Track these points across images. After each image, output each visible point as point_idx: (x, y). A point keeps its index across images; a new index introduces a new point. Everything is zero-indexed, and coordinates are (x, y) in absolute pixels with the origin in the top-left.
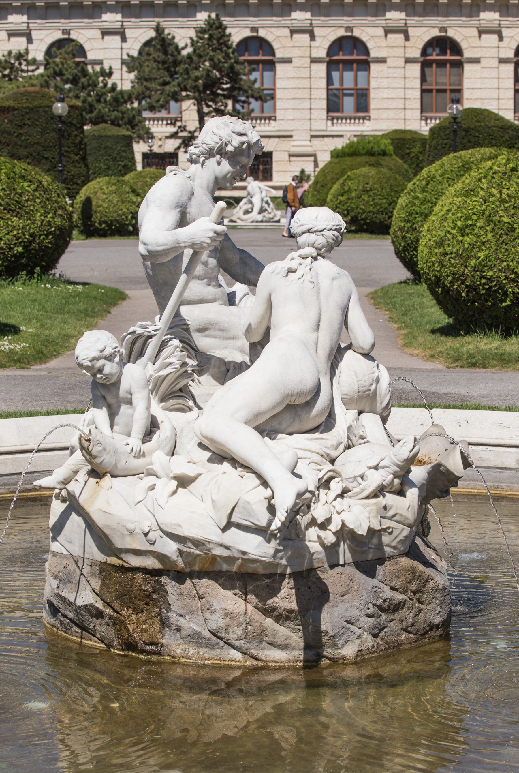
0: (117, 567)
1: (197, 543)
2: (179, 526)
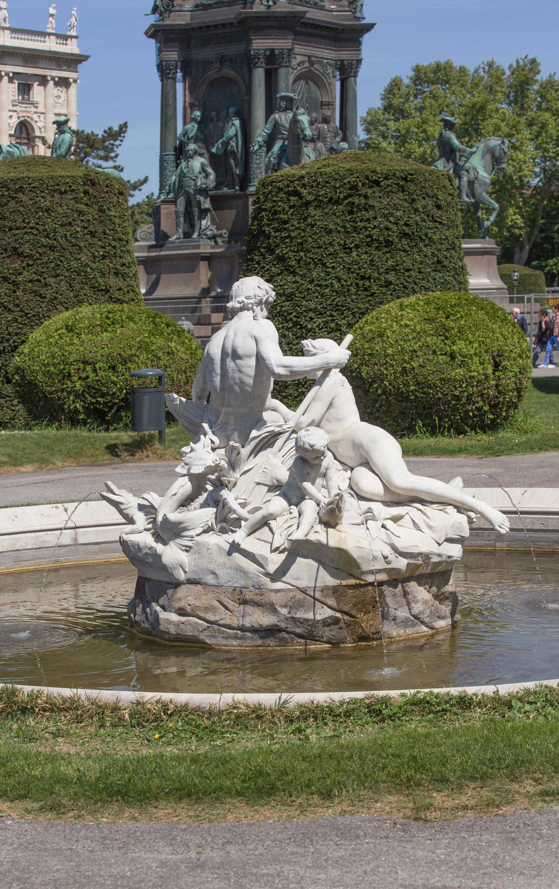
0: (353, 586)
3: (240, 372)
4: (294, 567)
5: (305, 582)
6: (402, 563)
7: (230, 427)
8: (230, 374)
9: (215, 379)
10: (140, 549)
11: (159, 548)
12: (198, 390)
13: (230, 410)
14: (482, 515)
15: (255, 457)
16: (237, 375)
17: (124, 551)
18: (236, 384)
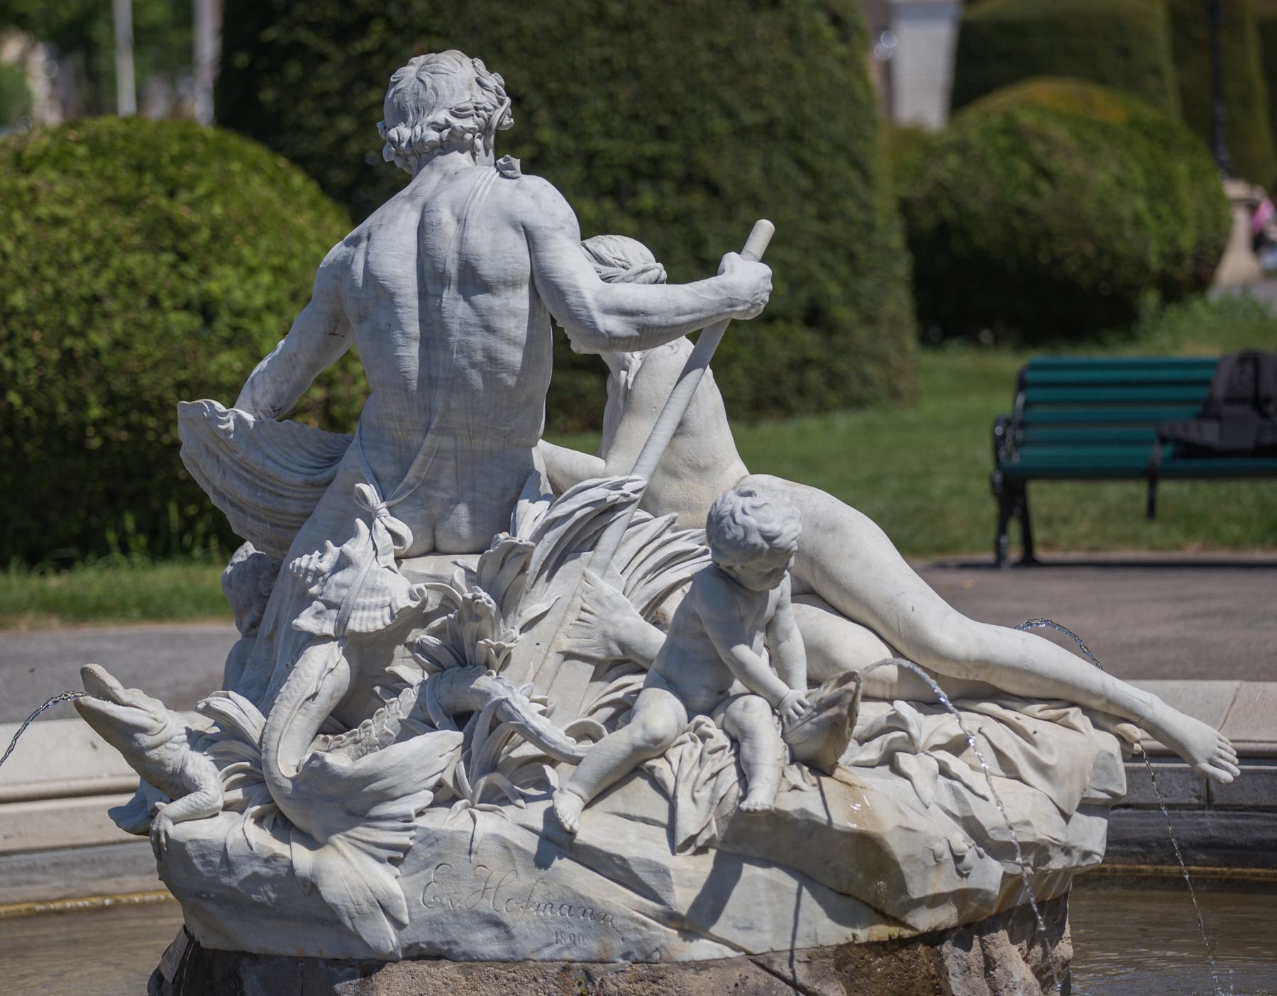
1: (1040, 850)
2: (1027, 823)
3: (489, 329)
4: (738, 892)
5: (764, 940)
6: (990, 875)
7: (441, 495)
8: (456, 337)
9: (402, 352)
10: (228, 863)
11: (302, 857)
12: (285, 387)
13: (446, 442)
14: (1154, 729)
15: (549, 579)
16: (478, 339)
17: (165, 874)
18: (473, 365)
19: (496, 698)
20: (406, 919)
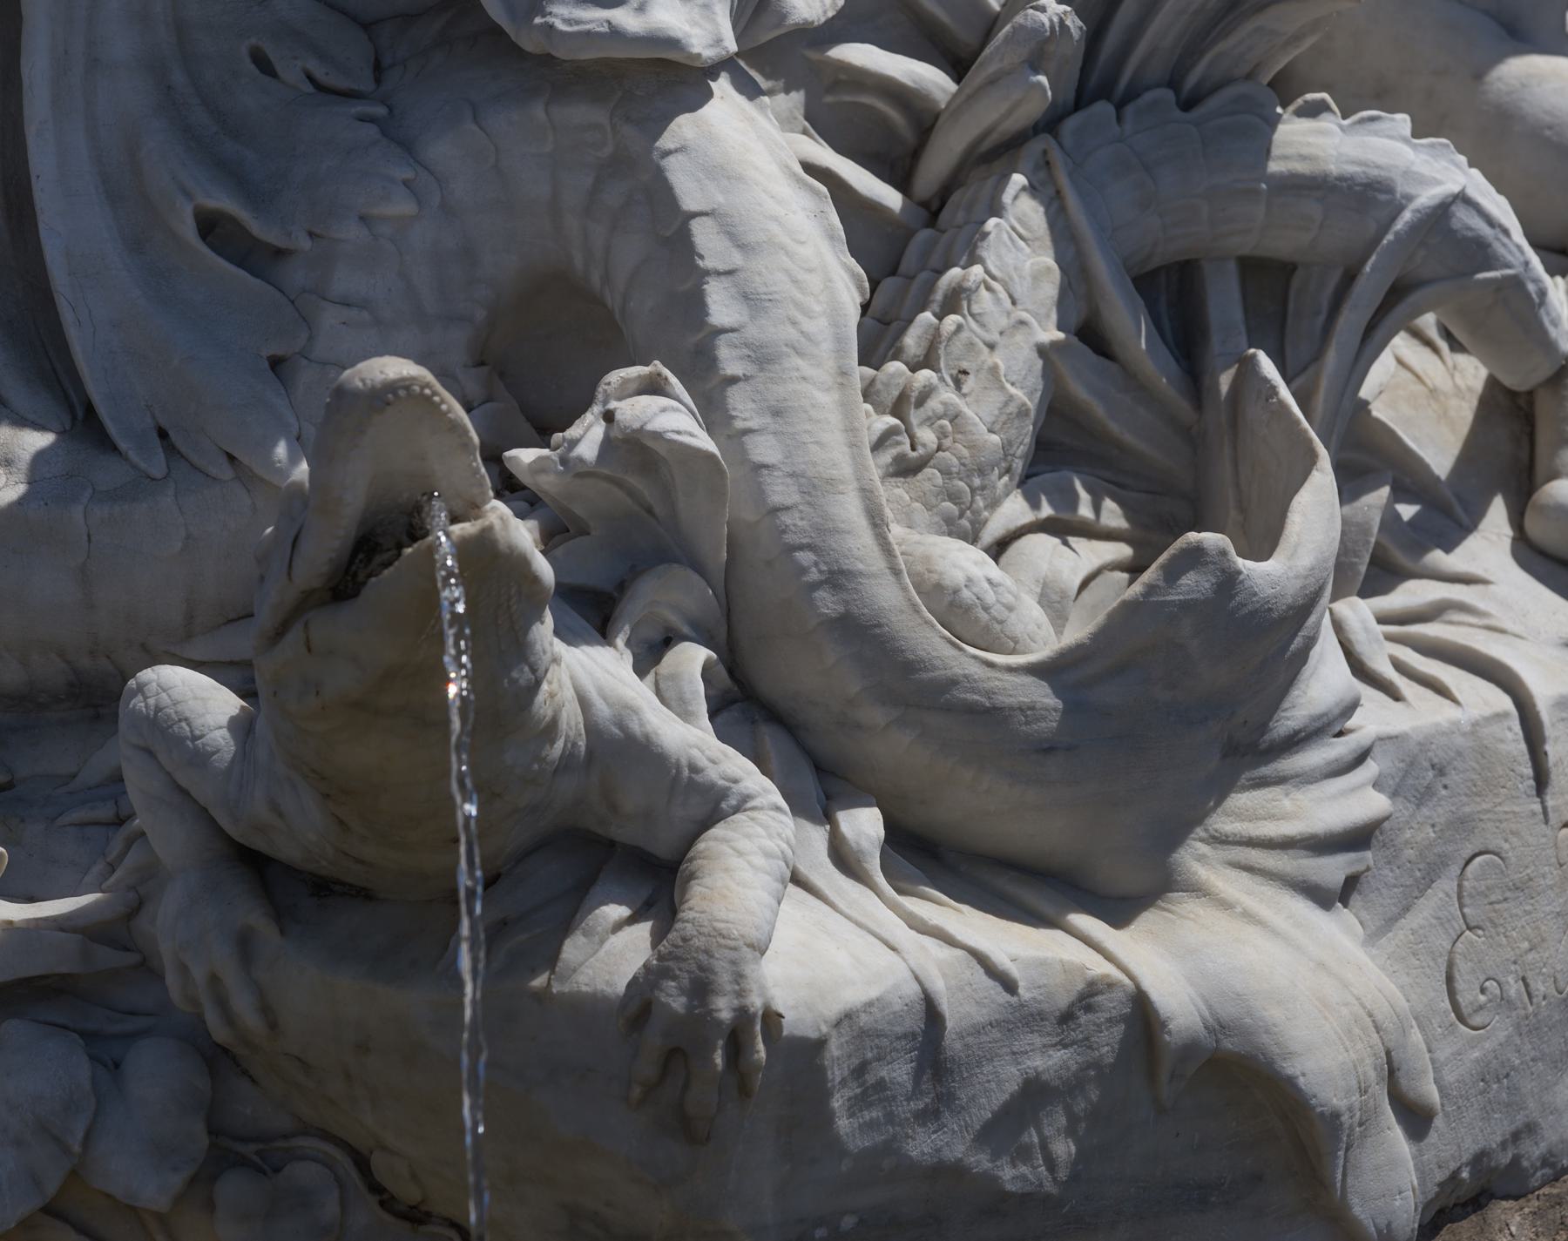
19: (1427, 197)
20: (1433, 1094)
